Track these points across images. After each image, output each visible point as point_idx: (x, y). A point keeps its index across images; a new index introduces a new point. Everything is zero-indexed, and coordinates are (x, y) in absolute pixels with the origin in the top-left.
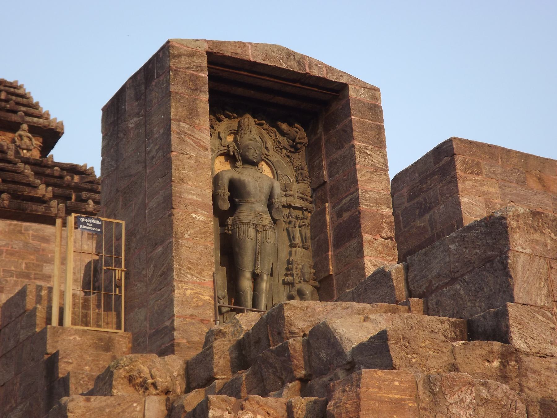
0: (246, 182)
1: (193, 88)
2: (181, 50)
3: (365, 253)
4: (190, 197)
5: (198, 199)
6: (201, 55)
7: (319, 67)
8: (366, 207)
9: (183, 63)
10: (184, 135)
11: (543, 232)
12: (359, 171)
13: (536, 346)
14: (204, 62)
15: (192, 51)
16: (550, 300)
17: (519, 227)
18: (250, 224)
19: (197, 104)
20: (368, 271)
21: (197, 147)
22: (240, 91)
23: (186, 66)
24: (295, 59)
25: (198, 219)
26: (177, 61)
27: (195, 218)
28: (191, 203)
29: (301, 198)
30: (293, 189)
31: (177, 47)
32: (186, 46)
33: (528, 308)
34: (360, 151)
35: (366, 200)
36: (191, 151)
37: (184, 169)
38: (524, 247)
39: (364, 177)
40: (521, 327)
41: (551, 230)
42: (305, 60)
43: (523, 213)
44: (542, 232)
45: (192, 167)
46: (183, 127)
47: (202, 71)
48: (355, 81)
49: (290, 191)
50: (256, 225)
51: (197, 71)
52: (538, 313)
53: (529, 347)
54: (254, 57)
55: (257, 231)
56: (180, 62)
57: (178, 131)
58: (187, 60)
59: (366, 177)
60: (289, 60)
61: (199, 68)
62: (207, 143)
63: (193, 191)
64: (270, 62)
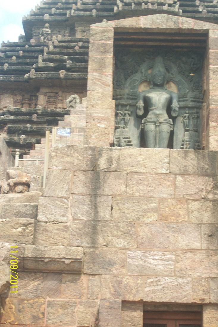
0: (151, 97)
1: (103, 51)
2: (97, 30)
3: (210, 134)
4: (97, 115)
5: (102, 115)
6: (110, 30)
7: (189, 22)
8: (214, 106)
9: (98, 38)
10: (96, 80)
11: (73, 156)
12: (211, 84)
13: (52, 218)
14: (112, 35)
15: (104, 29)
16: (68, 193)
17: (56, 156)
18: (152, 122)
19: (105, 61)
20: (211, 145)
21: (104, 86)
22: (150, 43)
23: (100, 39)
24: (172, 20)
25: (101, 127)
26: (94, 37)
27: (99, 127)
28: (97, 118)
29: (195, 101)
30: (188, 96)
31: (94, 29)
32: (101, 27)
33: (52, 199)
34: (214, 71)
35: (215, 101)
36: (99, 89)
37: (94, 99)
38: (58, 166)
39: (214, 87)
40: (45, 209)
41: (79, 154)
42: (179, 20)
43: (61, 148)
44: (72, 156)
45: (99, 98)
46: (95, 75)
47: (110, 40)
48: (214, 26)
49: (186, 97)
50: (155, 123)
51: (106, 41)
52: (58, 200)
53: (48, 219)
54: (144, 25)
55: (156, 126)
56: (96, 37)
57: (92, 78)
58: (101, 35)
59: (216, 87)
60: (168, 22)
61: (108, 39)
62: (110, 82)
63: (99, 111)
64: (155, 26)
